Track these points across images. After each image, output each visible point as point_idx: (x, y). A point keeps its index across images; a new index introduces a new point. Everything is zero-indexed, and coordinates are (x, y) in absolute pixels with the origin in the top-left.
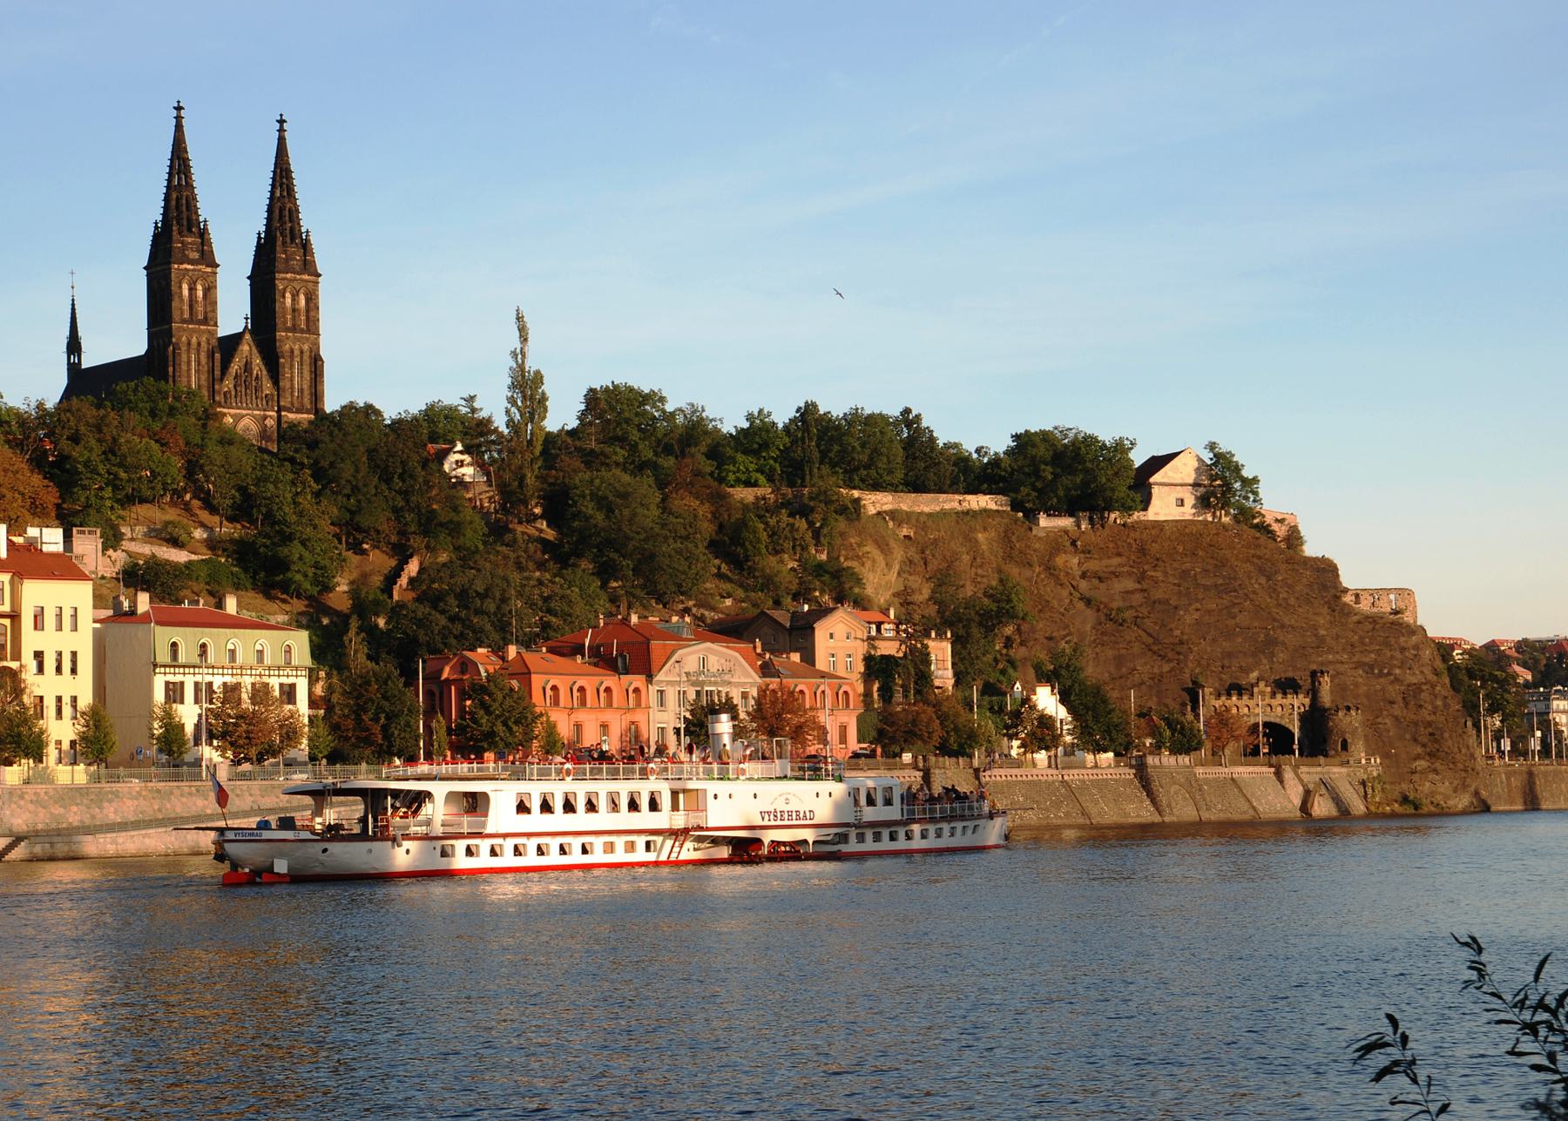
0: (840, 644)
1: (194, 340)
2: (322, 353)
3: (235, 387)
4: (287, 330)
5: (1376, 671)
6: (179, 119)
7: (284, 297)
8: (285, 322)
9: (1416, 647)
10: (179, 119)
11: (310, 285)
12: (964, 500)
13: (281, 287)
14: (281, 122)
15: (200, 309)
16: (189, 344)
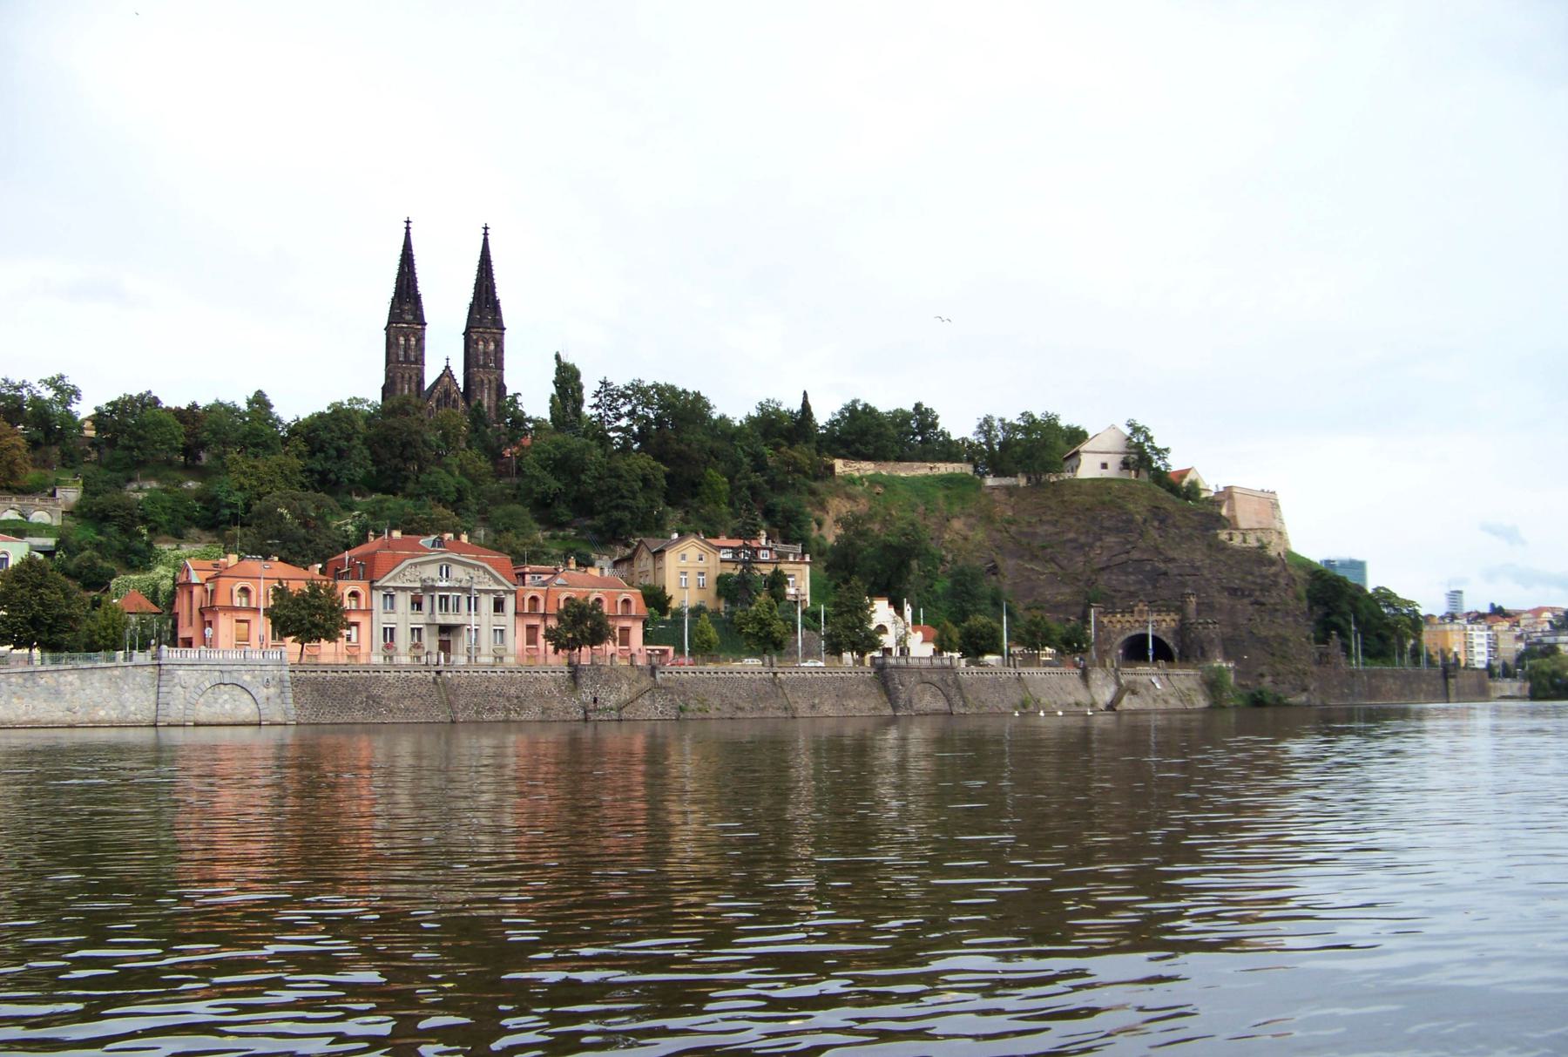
0: (691, 565)
1: (407, 375)
2: (506, 382)
3: (437, 406)
4: (478, 366)
5: (1239, 593)
6: (408, 228)
7: (477, 344)
8: (478, 360)
9: (1276, 575)
10: (408, 228)
11: (498, 336)
12: (935, 467)
13: (475, 337)
14: (486, 228)
15: (412, 354)
16: (403, 377)
